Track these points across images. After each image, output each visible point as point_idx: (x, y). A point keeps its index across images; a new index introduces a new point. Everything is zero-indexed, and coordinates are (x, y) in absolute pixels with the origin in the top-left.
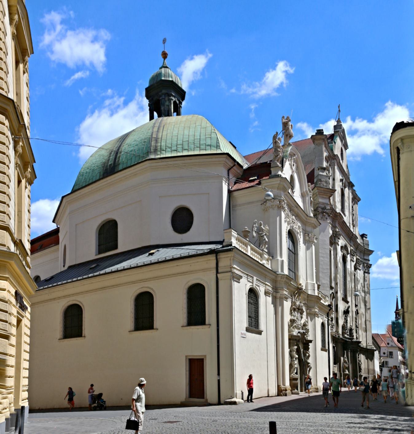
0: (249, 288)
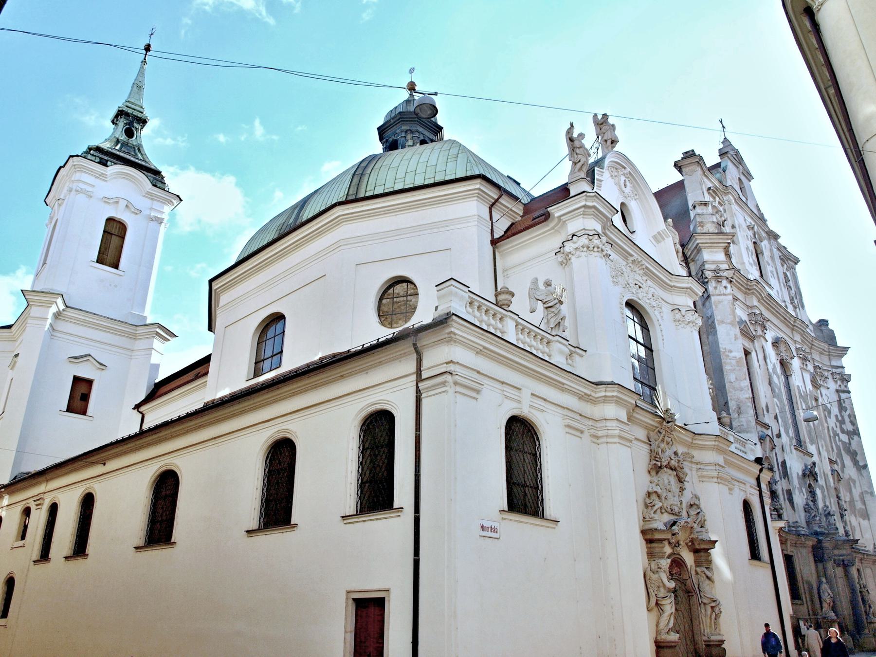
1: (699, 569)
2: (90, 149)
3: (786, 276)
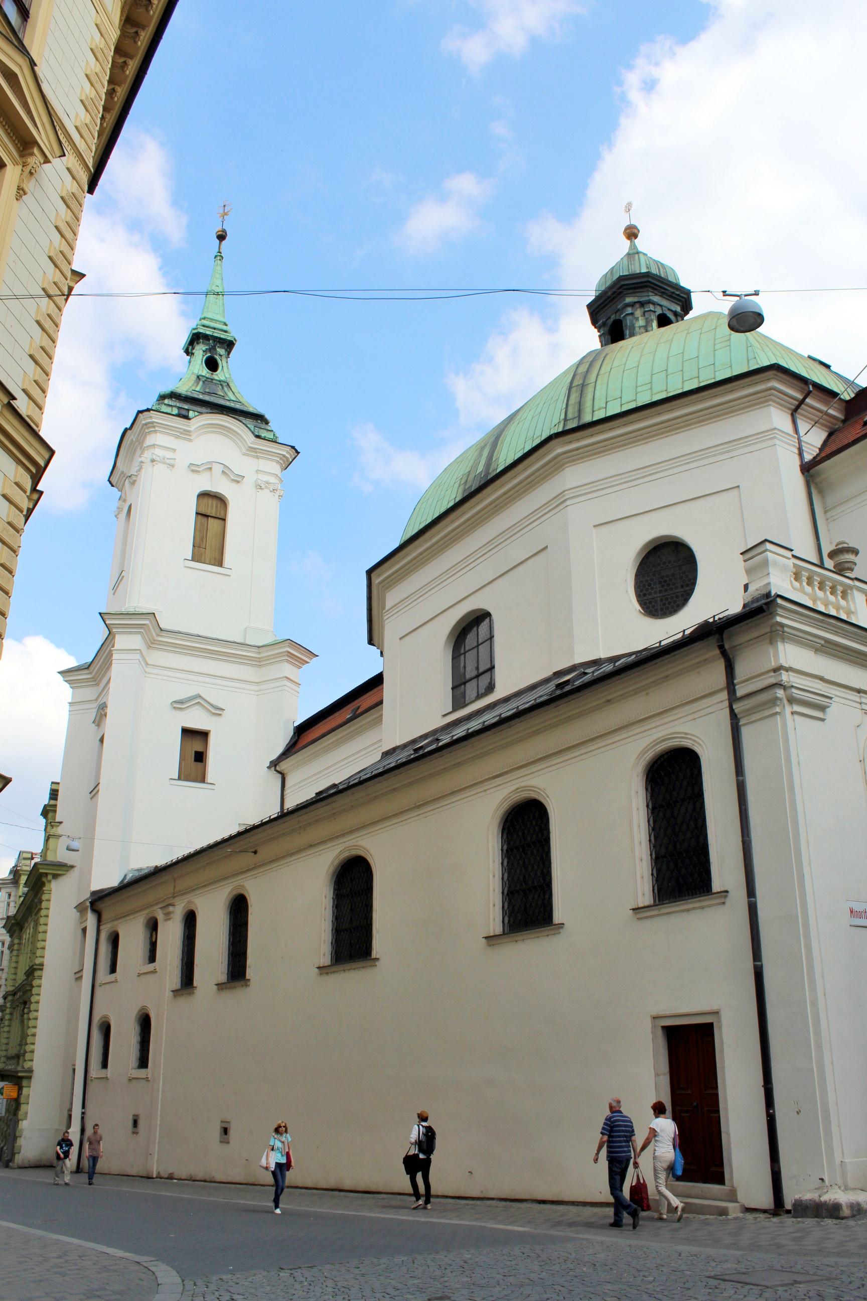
2: (162, 397)
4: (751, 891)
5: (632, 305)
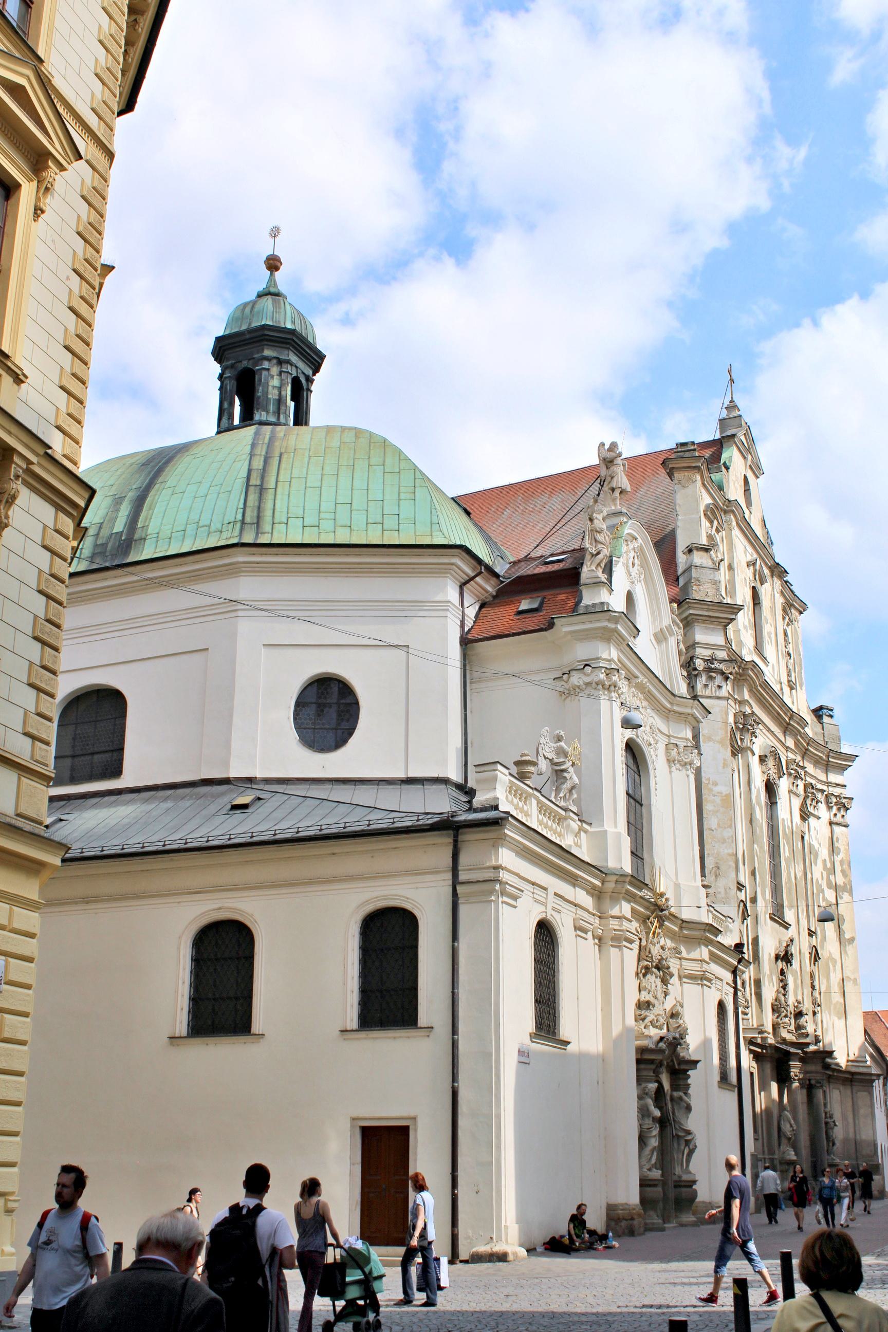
0: (537, 920)
1: (676, 1094)
3: (785, 634)
4: (454, 1031)
5: (269, 359)
